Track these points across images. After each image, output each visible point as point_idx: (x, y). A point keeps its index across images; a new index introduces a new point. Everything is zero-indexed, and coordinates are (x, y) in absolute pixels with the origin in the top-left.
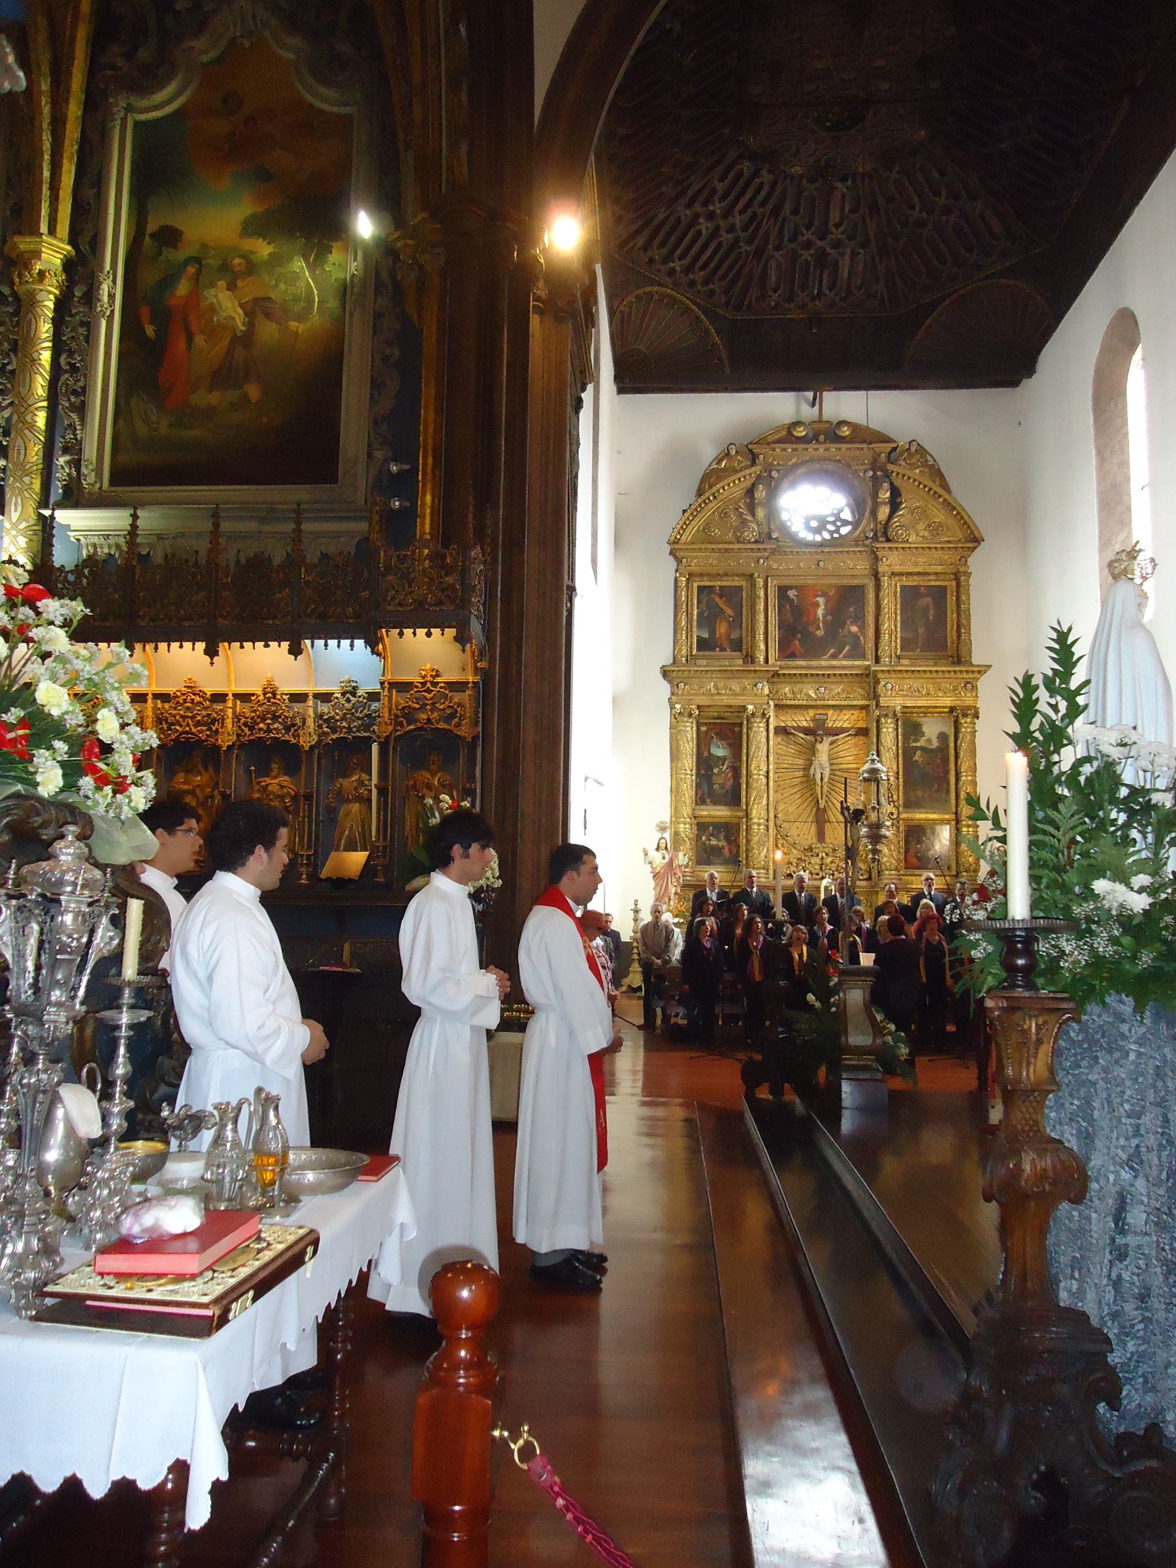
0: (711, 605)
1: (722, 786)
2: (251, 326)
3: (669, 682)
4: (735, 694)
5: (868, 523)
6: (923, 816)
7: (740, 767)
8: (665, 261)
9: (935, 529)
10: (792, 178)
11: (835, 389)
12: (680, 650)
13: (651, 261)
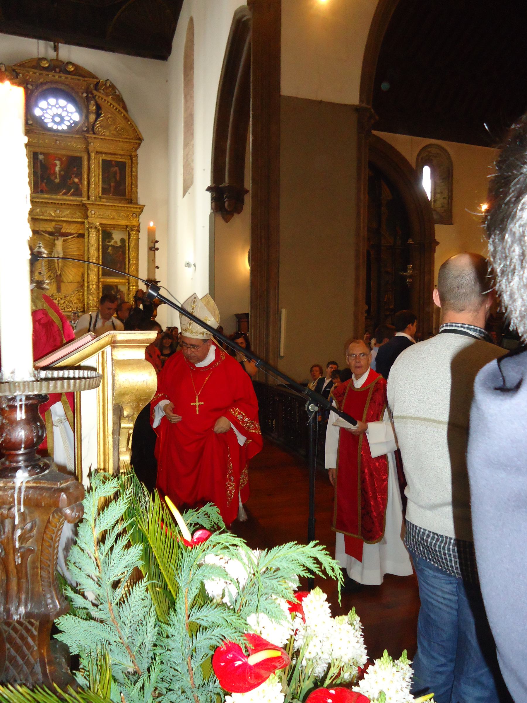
6: (111, 280)
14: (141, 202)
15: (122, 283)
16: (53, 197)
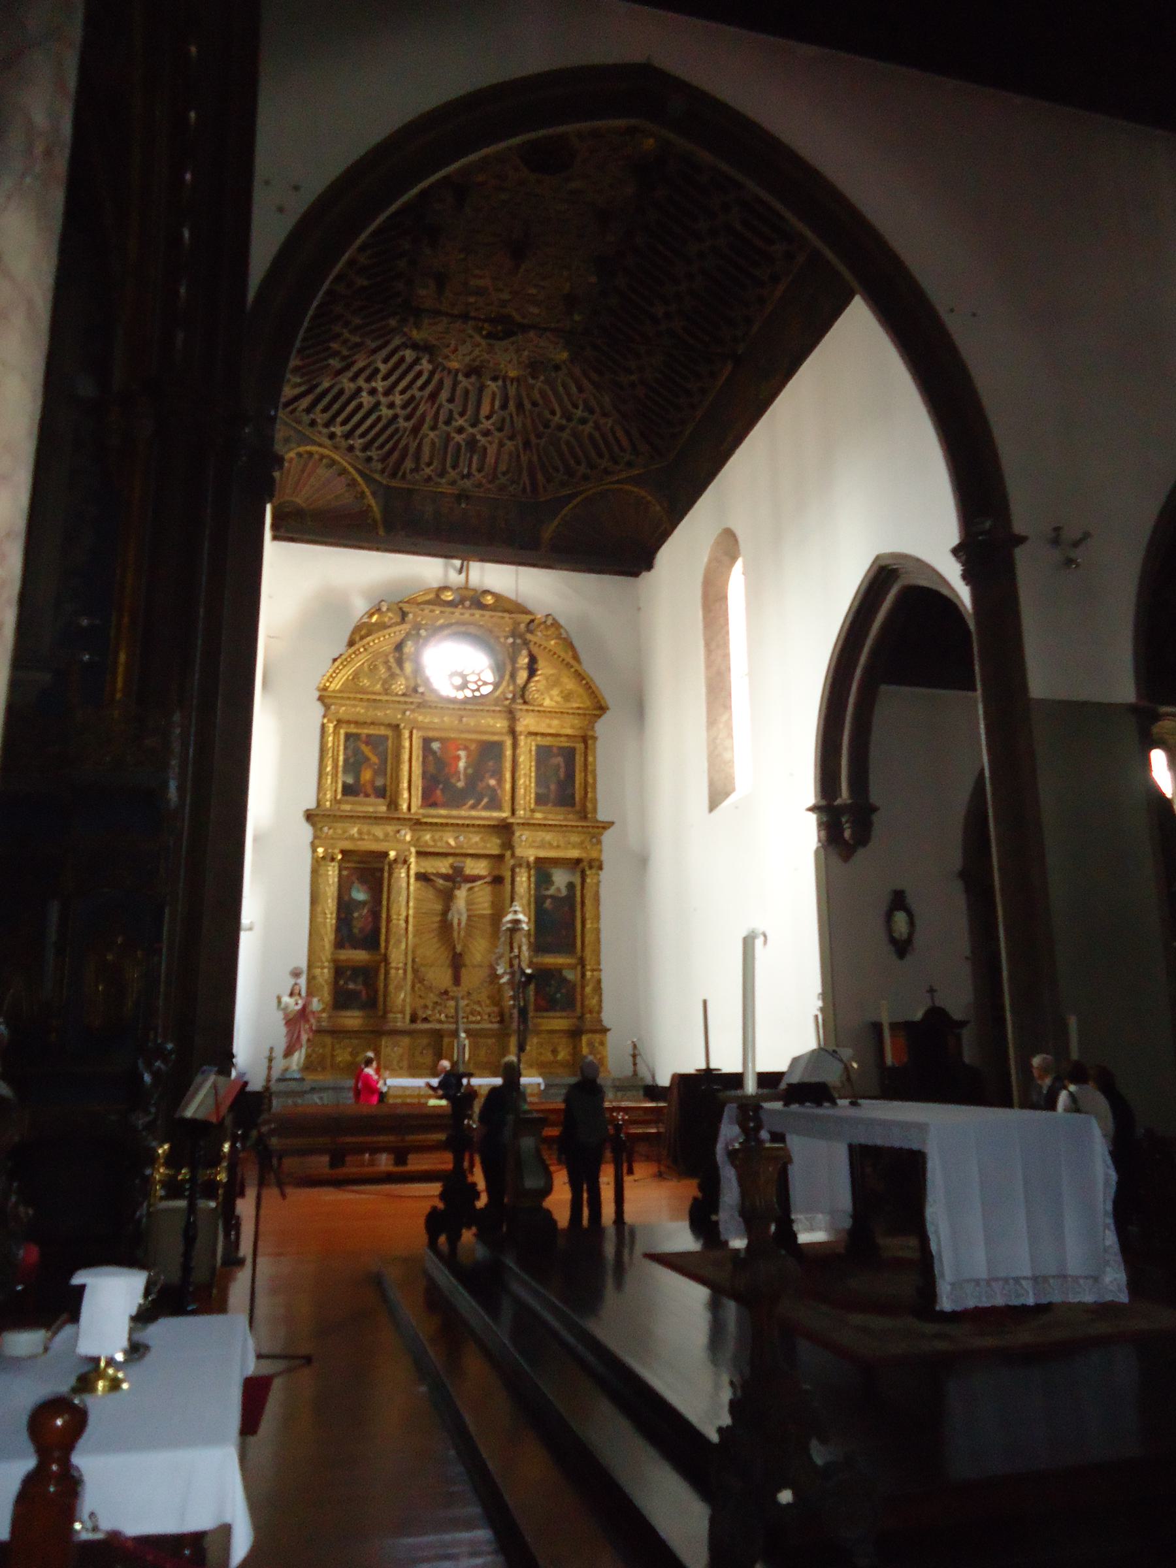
0: (357, 752)
1: (361, 930)
3: (313, 825)
4: (377, 839)
5: (508, 686)
7: (380, 912)
8: (327, 425)
9: (567, 697)
10: (449, 372)
11: (483, 560)
12: (325, 794)
13: (313, 423)
14: (602, 816)
15: (569, 965)
16: (454, 813)
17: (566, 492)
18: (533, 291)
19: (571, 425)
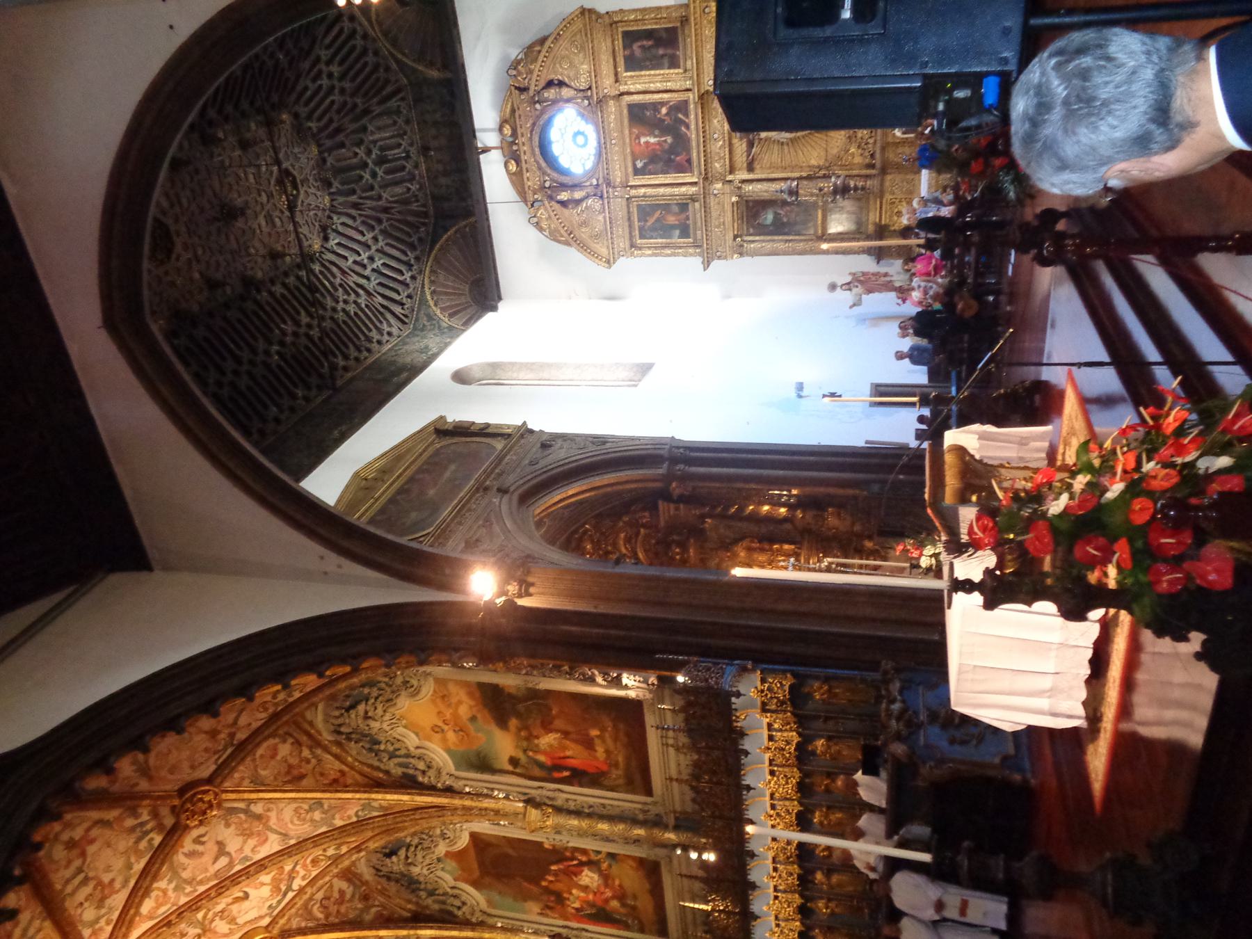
0: (653, 229)
2: (557, 731)
13: (409, 296)
16: (694, 144)
17: (394, 66)
18: (251, 177)
19: (336, 83)
